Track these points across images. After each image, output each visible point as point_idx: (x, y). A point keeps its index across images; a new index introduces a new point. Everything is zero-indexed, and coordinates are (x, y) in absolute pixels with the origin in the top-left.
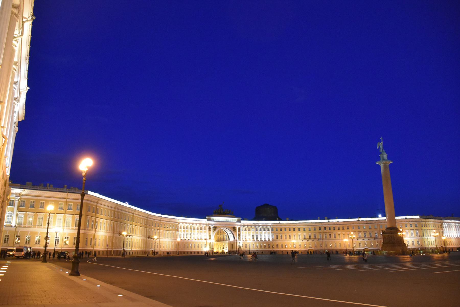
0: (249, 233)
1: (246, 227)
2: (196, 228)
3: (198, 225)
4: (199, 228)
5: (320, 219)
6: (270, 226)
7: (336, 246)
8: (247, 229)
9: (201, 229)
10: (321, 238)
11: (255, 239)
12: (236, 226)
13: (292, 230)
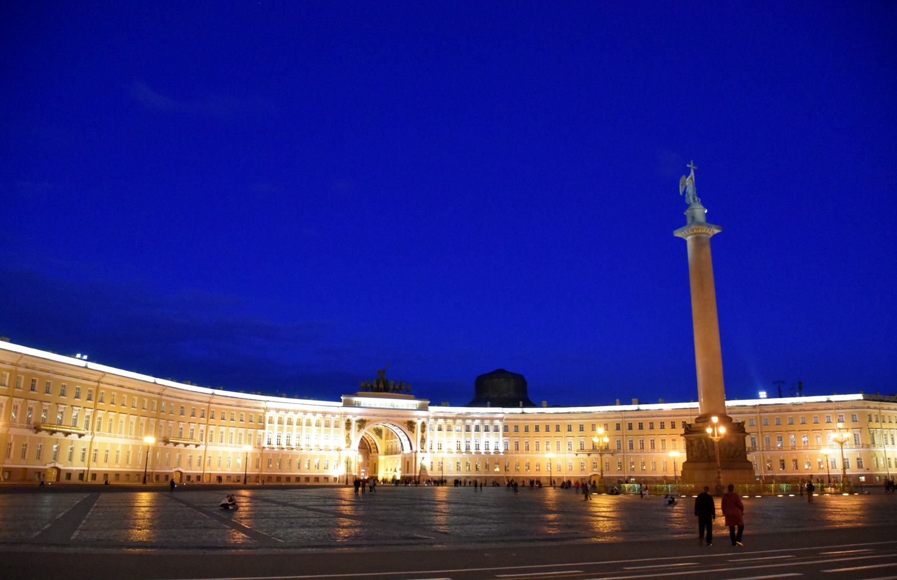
0: (448, 435)
1: (441, 421)
2: (314, 422)
3: (319, 416)
4: (323, 423)
5: (621, 404)
6: (501, 419)
8: (444, 427)
9: (327, 425)
11: (463, 449)
12: (415, 420)
13: (553, 429)
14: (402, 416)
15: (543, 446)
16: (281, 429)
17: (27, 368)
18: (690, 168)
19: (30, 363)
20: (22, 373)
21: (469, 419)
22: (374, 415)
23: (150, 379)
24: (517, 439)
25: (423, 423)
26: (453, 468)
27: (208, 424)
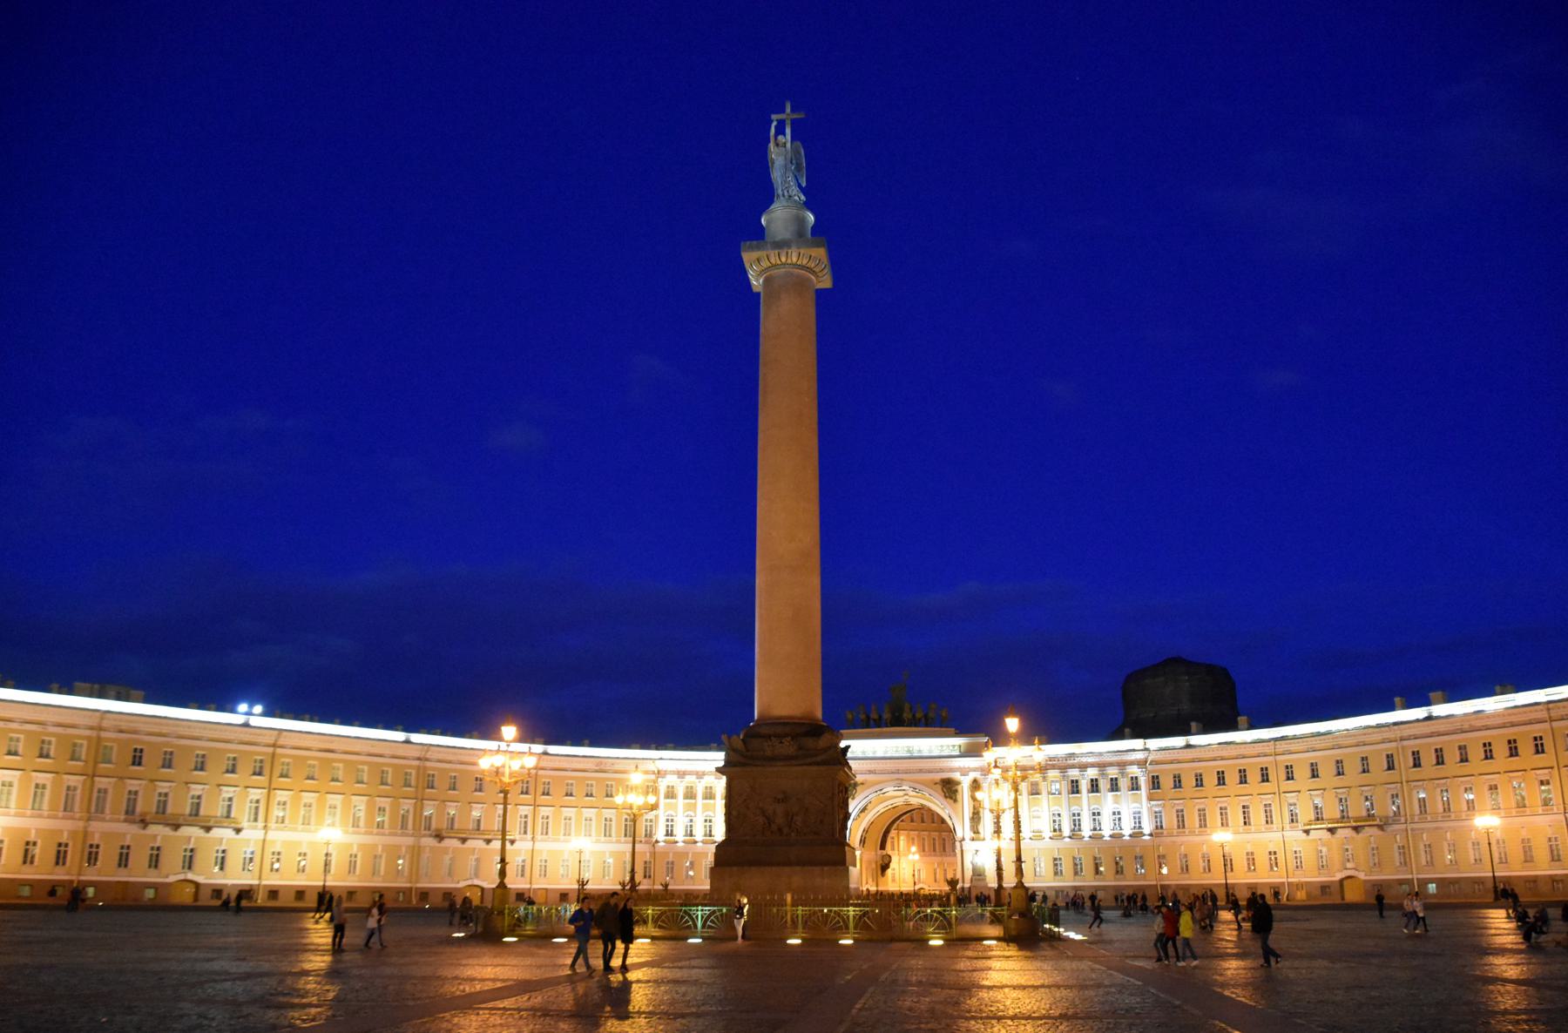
6: (1142, 764)
11: (1066, 831)
12: (957, 776)
13: (1254, 777)
14: (930, 771)
15: (1214, 817)
16: (694, 808)
17: (121, 731)
18: (783, 111)
19: (127, 725)
20: (114, 740)
21: (1073, 766)
22: (870, 772)
23: (399, 736)
24: (1179, 804)
25: (975, 781)
26: (1045, 868)
27: (535, 805)
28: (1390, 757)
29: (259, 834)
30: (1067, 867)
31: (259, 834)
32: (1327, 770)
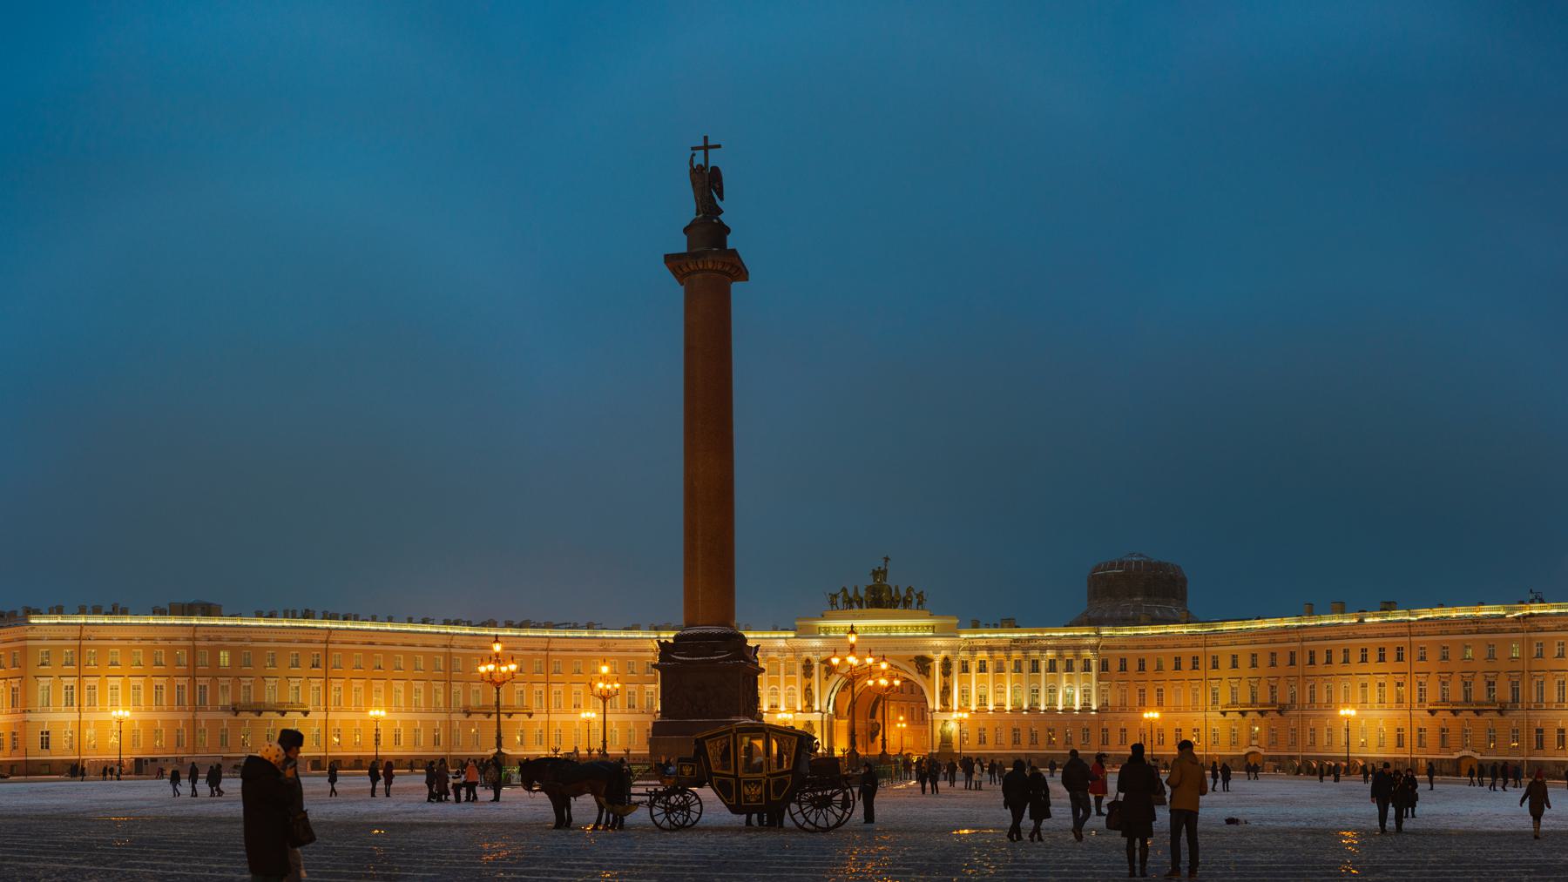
6: (1094, 648)
7: (1330, 744)
10: (1515, 700)
12: (930, 654)
21: (1034, 648)
25: (946, 659)
28: (1292, 654)
29: (322, 716)
30: (1025, 738)
31: (322, 716)
32: (1244, 662)
